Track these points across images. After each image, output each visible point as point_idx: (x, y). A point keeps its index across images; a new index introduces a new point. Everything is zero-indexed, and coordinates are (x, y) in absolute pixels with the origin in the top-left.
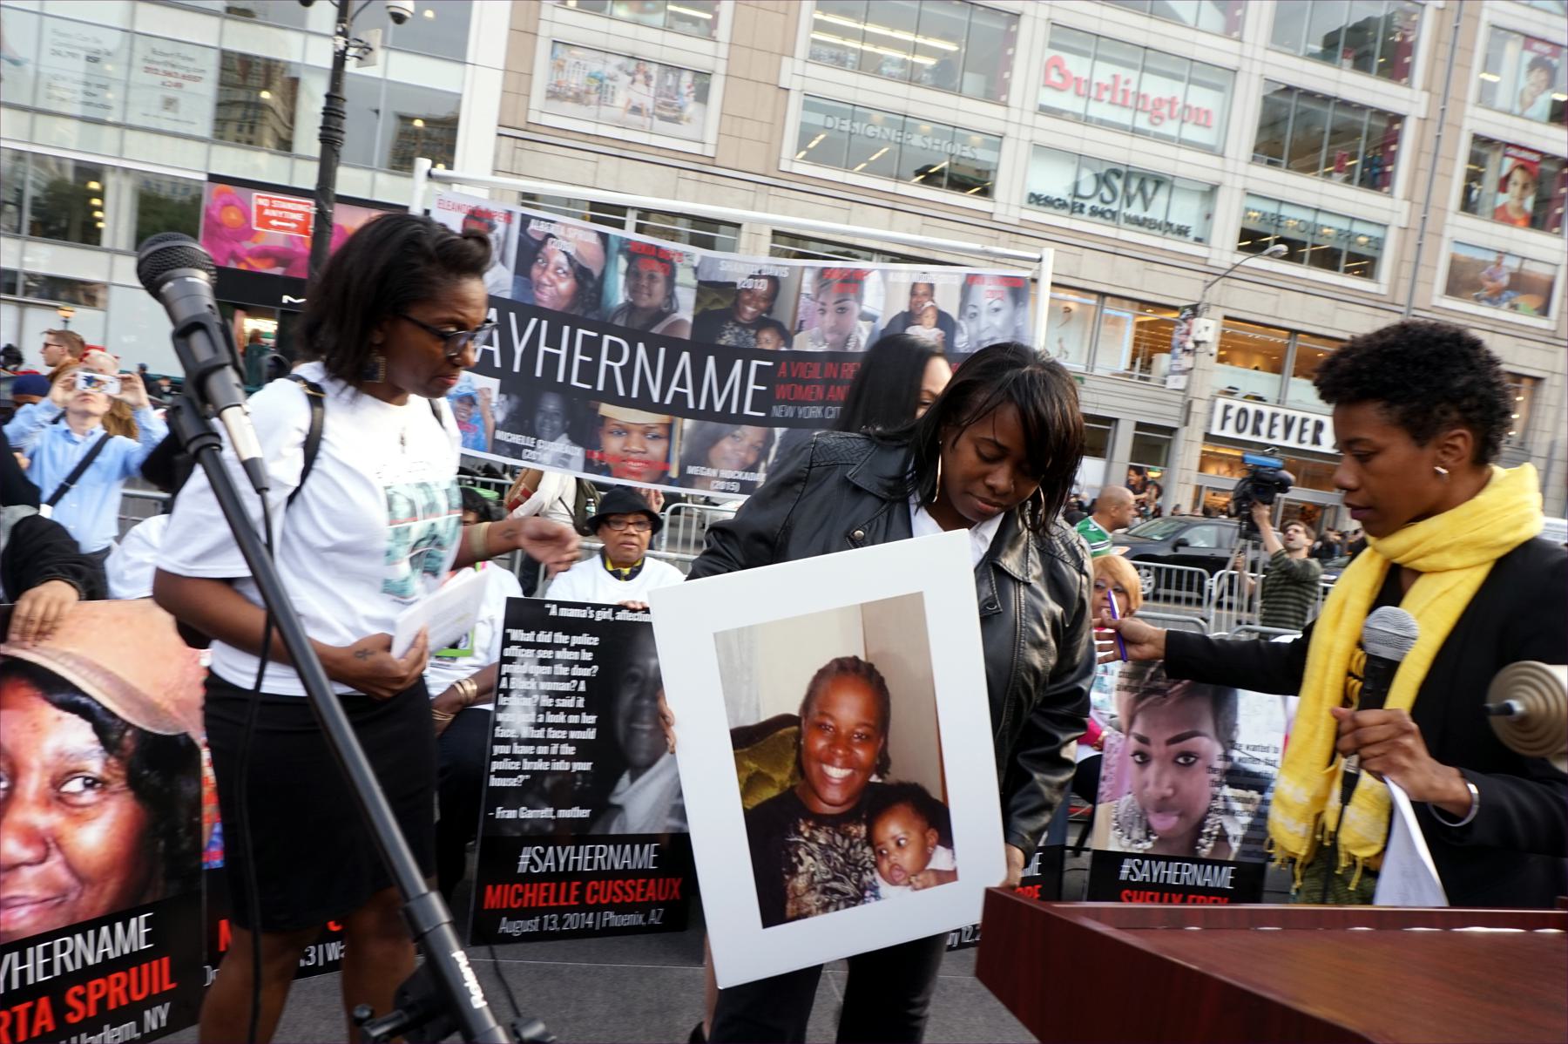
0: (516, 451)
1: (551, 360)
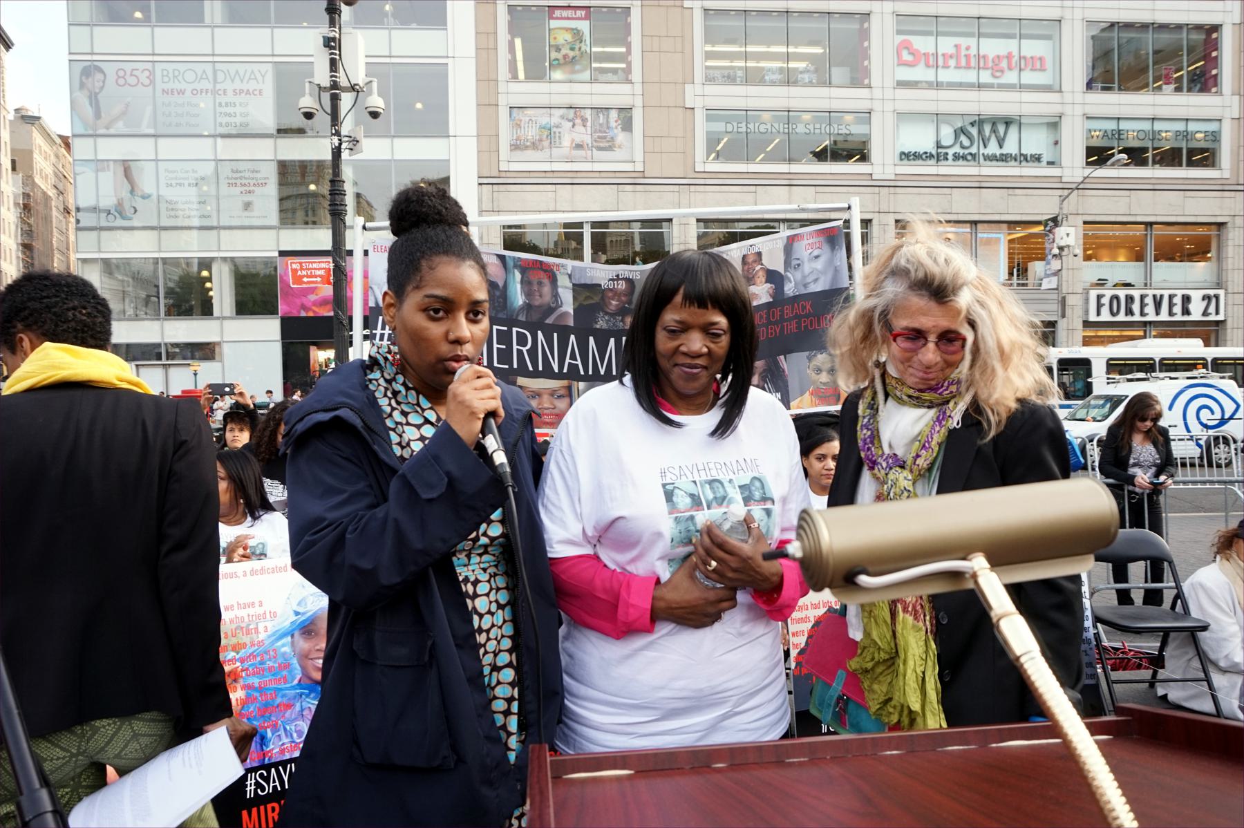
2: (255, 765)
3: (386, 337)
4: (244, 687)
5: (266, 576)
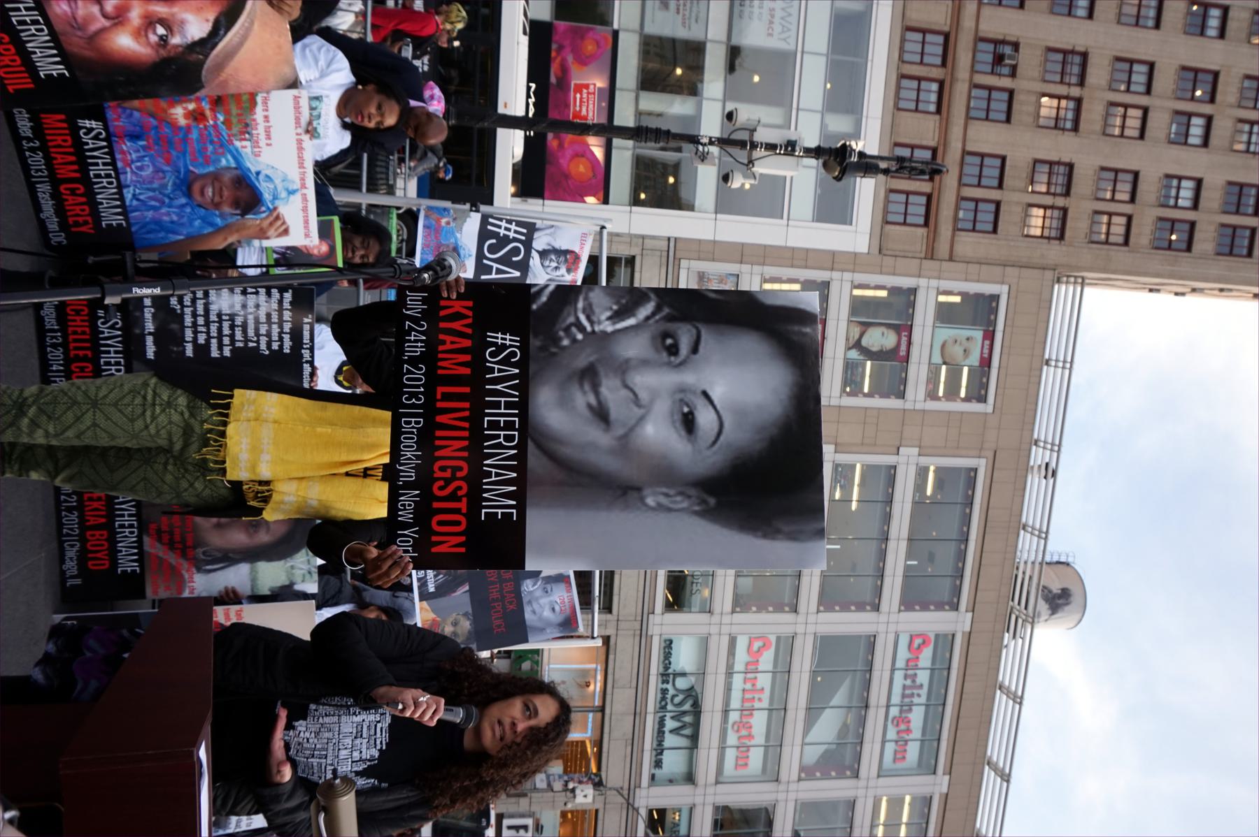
2: (111, 129)
4: (188, 129)
5: (295, 152)
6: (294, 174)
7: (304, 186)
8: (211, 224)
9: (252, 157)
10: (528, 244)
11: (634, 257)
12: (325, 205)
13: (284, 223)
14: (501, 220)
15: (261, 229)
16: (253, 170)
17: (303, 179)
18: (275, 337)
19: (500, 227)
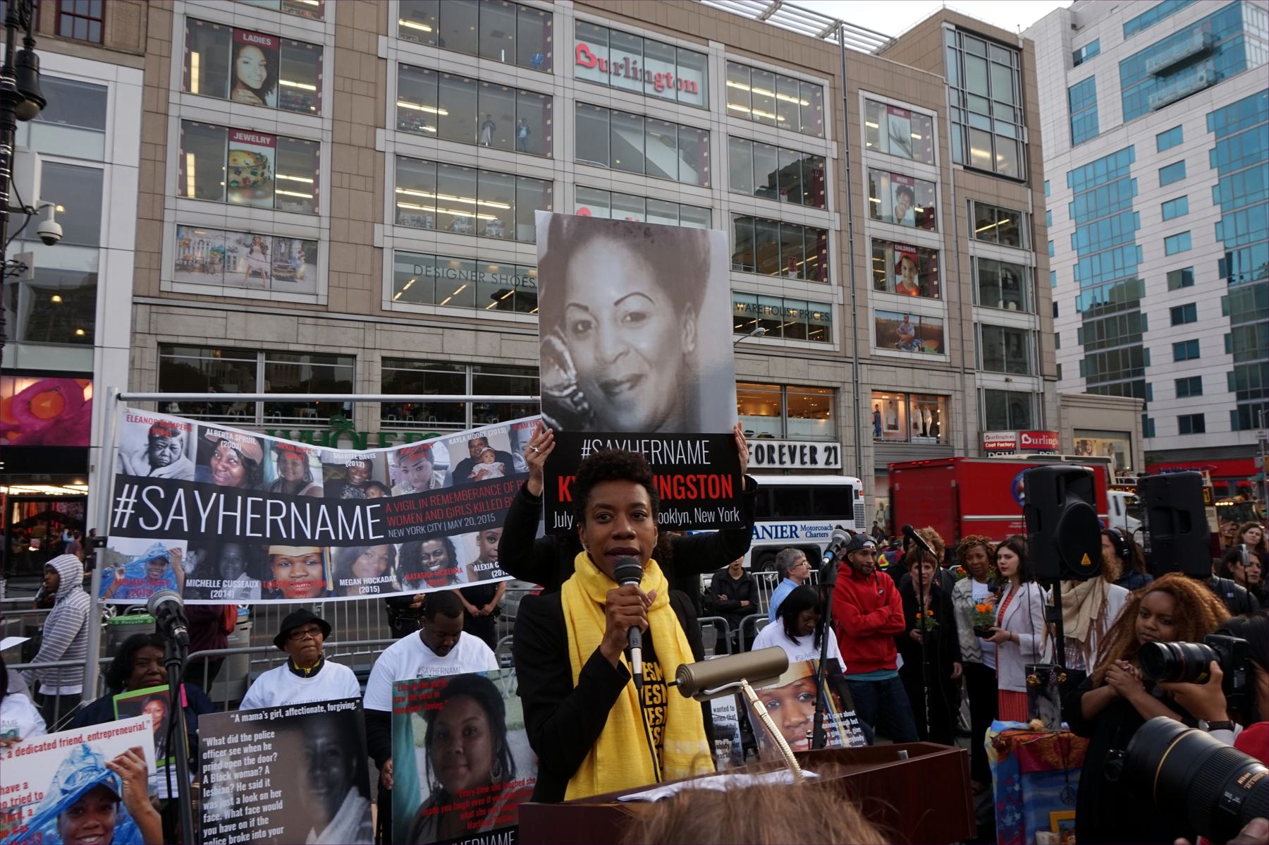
0: (205, 593)
1: (230, 521)
3: (130, 506)
5: (33, 755)
6: (64, 752)
7: (79, 740)
8: (131, 830)
9: (44, 802)
10: (143, 482)
11: (160, 344)
12: (100, 713)
13: (126, 755)
14: (114, 514)
15: (134, 777)
16: (60, 797)
17: (70, 742)
18: (259, 748)
19: (123, 515)
